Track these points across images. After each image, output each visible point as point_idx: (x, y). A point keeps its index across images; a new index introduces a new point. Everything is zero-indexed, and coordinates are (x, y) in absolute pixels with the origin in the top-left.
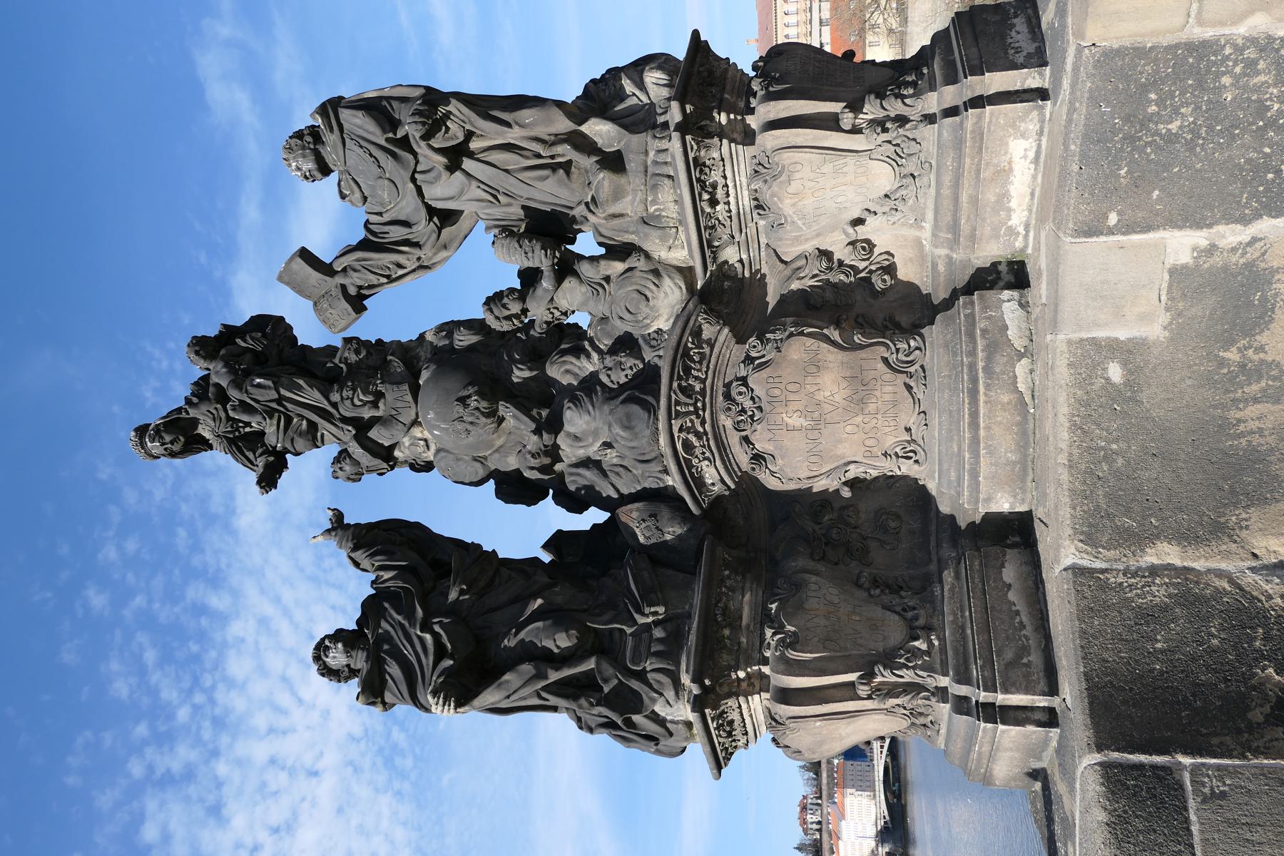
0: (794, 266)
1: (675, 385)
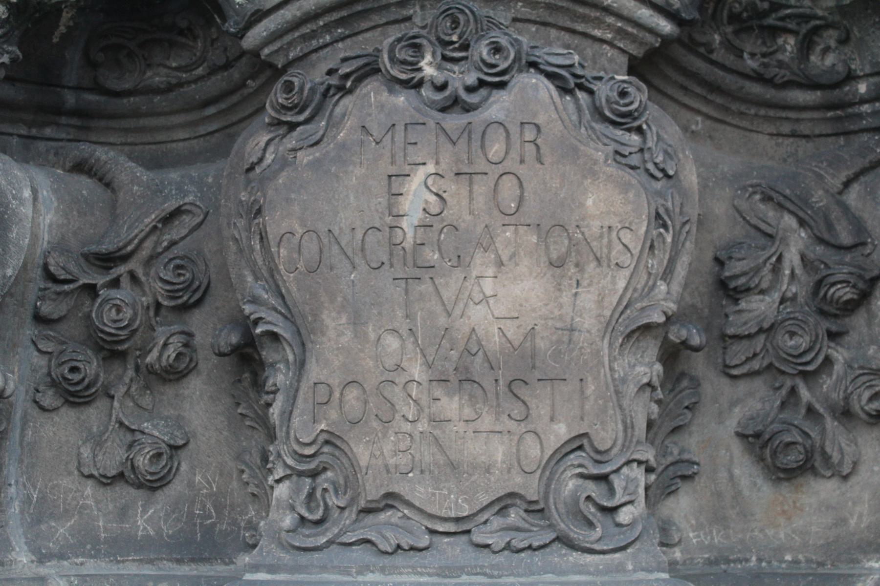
0: (835, 213)
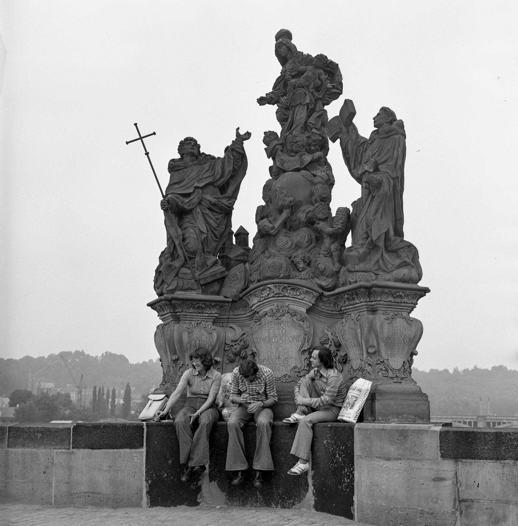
1: (286, 285)
